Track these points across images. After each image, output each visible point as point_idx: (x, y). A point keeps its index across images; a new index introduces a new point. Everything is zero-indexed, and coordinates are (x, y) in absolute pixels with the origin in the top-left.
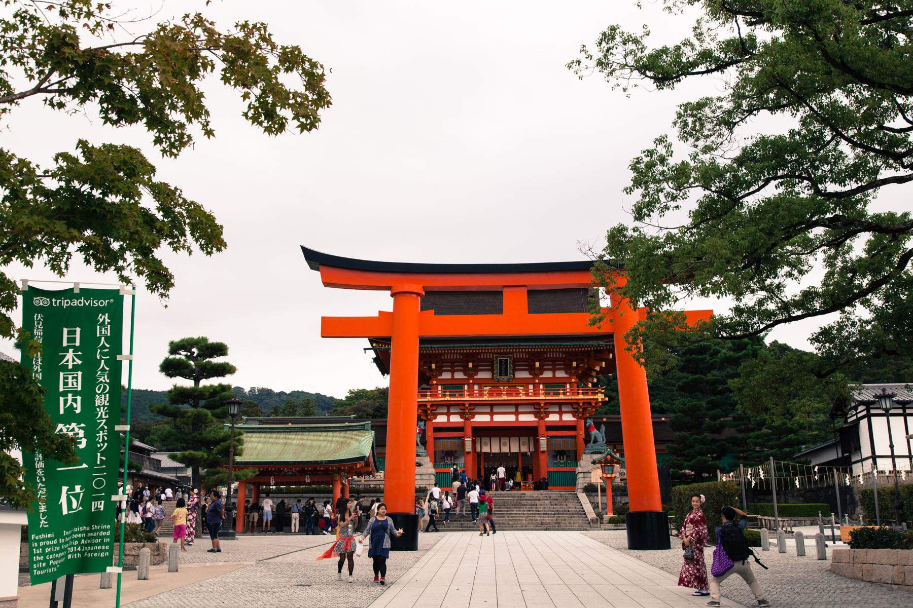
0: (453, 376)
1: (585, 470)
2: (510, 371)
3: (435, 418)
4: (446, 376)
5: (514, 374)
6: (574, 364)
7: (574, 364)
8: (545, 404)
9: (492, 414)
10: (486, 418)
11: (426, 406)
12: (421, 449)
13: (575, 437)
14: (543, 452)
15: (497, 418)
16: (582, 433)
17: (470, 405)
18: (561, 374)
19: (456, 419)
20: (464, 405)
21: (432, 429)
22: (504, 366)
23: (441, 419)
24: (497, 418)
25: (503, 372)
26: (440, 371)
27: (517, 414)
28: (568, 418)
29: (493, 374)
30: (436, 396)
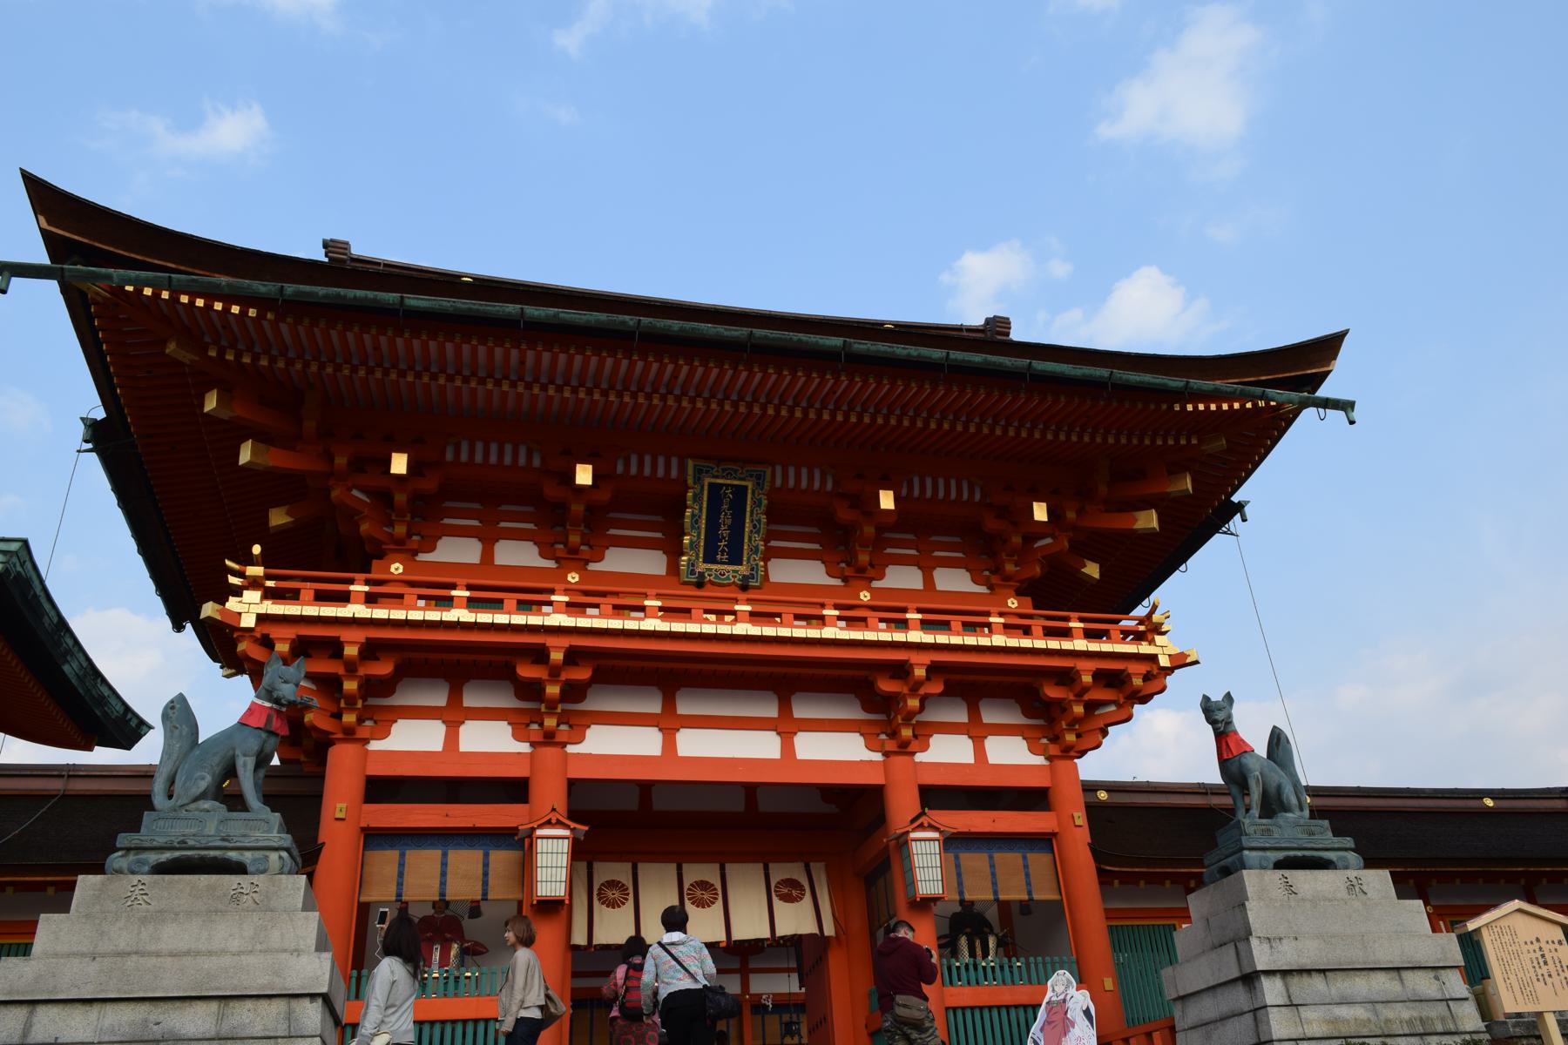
0: (488, 555)
1: (1287, 956)
2: (752, 539)
3: (385, 734)
4: (458, 551)
5: (766, 559)
6: (1040, 512)
7: (1040, 512)
8: (934, 669)
9: (669, 724)
10: (642, 743)
11: (334, 648)
12: (264, 828)
13: (1044, 841)
14: (927, 903)
15: (695, 744)
16: (1080, 818)
17: (573, 657)
18: (954, 581)
19: (490, 740)
20: (539, 655)
21: (356, 787)
22: (726, 519)
23: (413, 739)
24: (695, 744)
25: (725, 544)
26: (425, 510)
27: (786, 728)
28: (1011, 753)
29: (673, 551)
30: (397, 599)
